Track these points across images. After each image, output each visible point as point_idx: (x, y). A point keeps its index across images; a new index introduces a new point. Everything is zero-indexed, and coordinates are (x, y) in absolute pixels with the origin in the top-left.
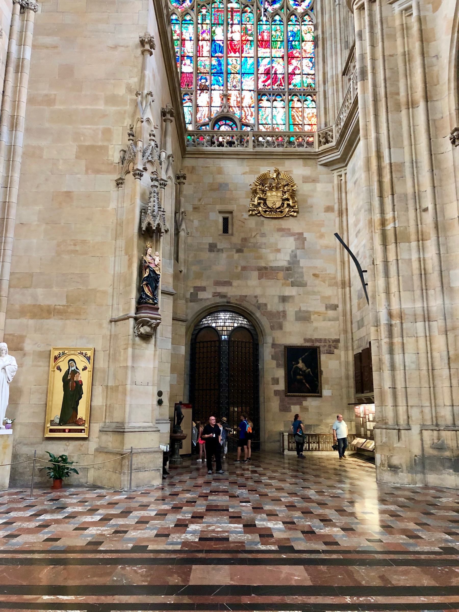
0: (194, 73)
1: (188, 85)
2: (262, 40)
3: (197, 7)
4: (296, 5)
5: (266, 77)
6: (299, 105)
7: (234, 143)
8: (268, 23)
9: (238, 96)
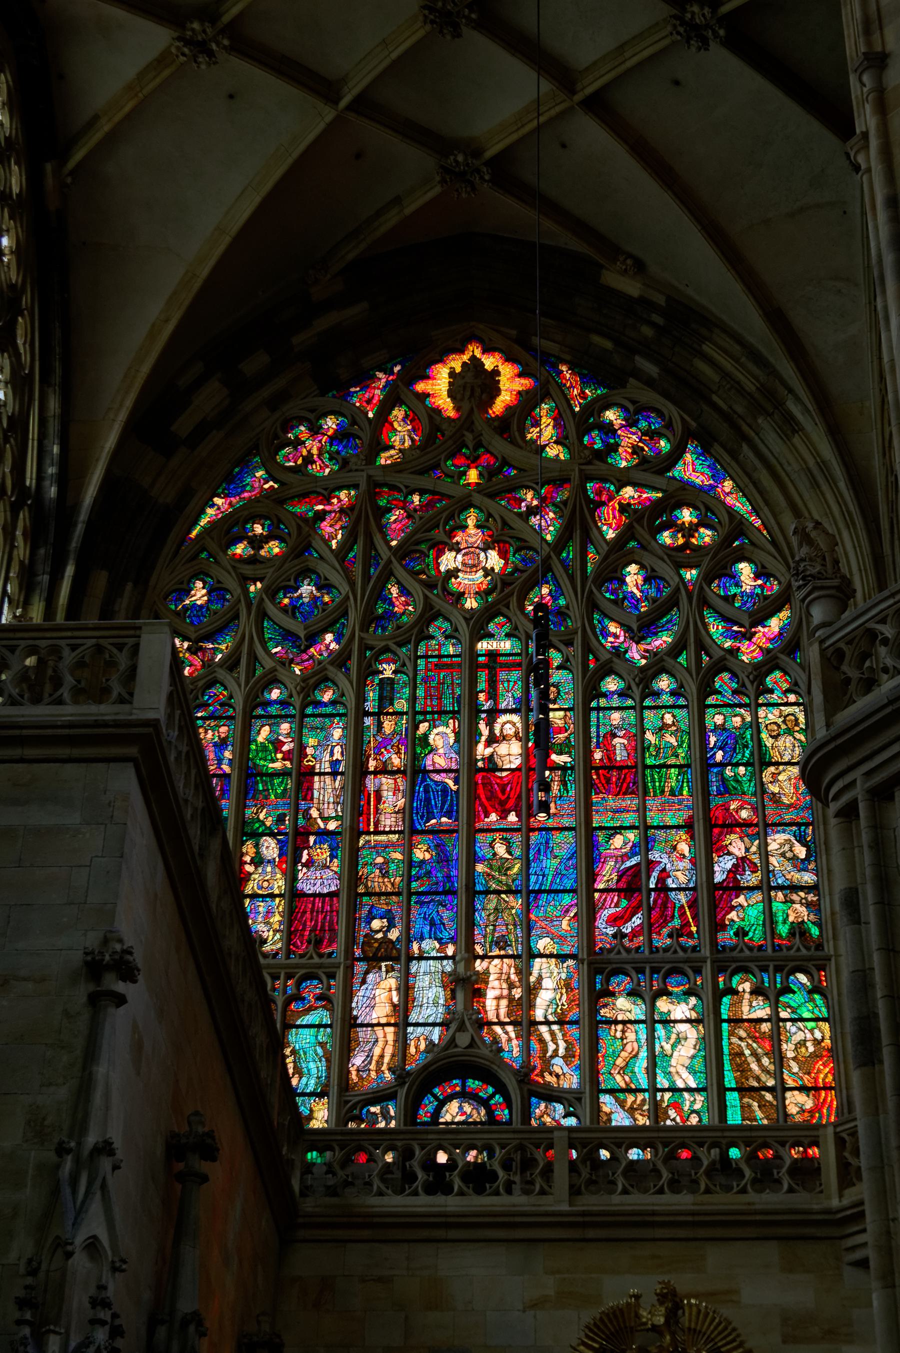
0: (344, 896)
1: (318, 943)
2: (610, 764)
4: (735, 636)
5: (624, 903)
7: (494, 1176)
8: (630, 702)
9: (513, 977)
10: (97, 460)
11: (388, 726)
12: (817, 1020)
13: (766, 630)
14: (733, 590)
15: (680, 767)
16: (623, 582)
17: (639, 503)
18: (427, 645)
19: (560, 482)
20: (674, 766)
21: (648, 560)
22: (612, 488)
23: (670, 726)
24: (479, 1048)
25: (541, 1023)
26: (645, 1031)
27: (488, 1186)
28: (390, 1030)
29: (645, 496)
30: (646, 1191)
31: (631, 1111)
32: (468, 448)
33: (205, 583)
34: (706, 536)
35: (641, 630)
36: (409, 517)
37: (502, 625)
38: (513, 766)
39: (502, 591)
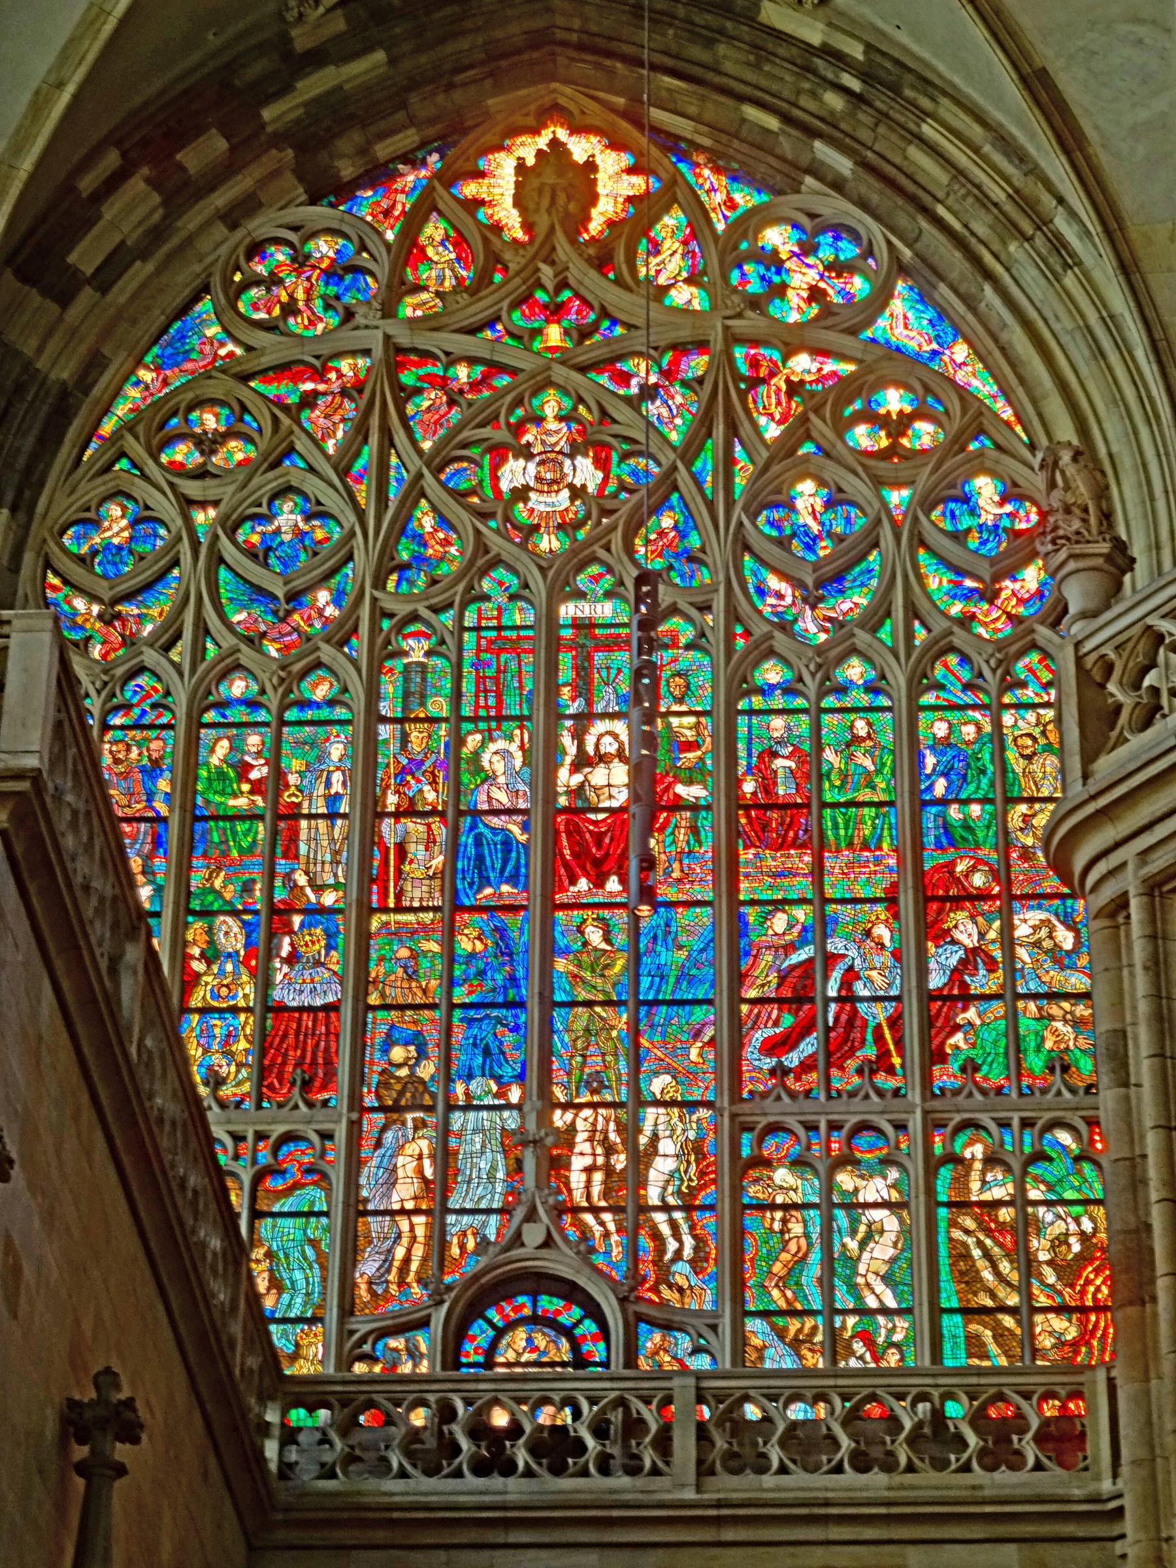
0: (347, 1012)
1: (306, 1086)
2: (766, 802)
3: (375, 629)
4: (968, 595)
5: (788, 1020)
7: (580, 1447)
8: (800, 703)
9: (613, 1136)
11: (416, 735)
12: (1086, 1202)
13: (1017, 586)
14: (965, 522)
15: (880, 804)
16: (792, 508)
17: (817, 381)
21: (833, 472)
22: (776, 356)
23: (863, 739)
26: (818, 1221)
28: (419, 1220)
29: (827, 369)
30: (814, 1469)
31: (796, 1345)
32: (544, 288)
33: (124, 509)
34: (924, 434)
37: (595, 579)
38: (615, 804)
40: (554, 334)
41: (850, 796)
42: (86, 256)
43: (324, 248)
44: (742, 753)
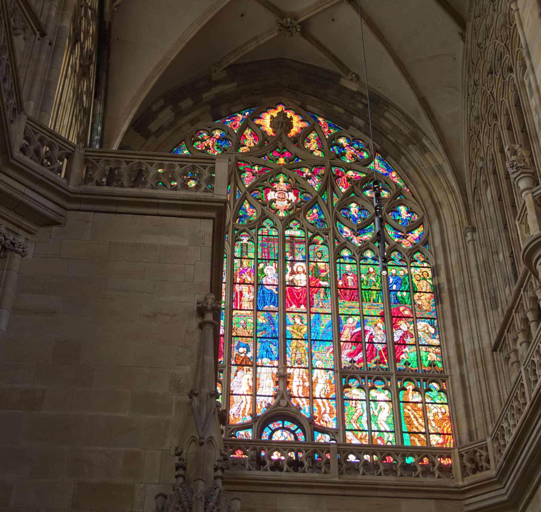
2: (345, 287)
3: (233, 233)
4: (399, 237)
5: (354, 348)
6: (417, 398)
7: (302, 464)
8: (354, 261)
9: (305, 377)
10: (118, 135)
11: (245, 263)
12: (442, 404)
13: (413, 235)
14: (398, 218)
17: (355, 178)
18: (262, 230)
19: (322, 166)
20: (375, 290)
24: (290, 407)
25: (318, 398)
26: (365, 404)
27: (300, 468)
29: (358, 175)
30: (373, 474)
35: (360, 230)
36: (253, 175)
37: (295, 225)
38: (303, 285)
39: (296, 210)
40: (282, 161)
41: (369, 288)
42: (153, 127)
43: (217, 133)
44: (338, 274)
